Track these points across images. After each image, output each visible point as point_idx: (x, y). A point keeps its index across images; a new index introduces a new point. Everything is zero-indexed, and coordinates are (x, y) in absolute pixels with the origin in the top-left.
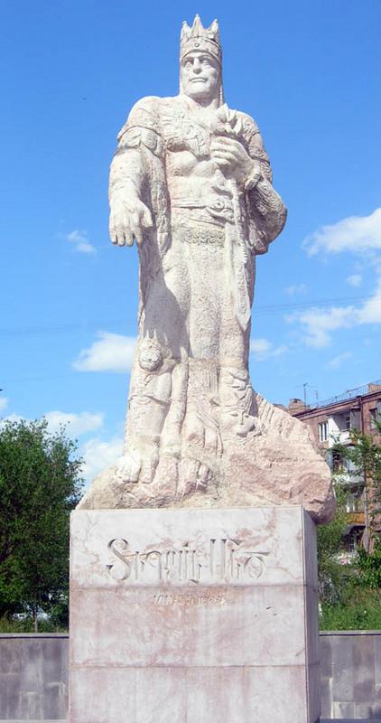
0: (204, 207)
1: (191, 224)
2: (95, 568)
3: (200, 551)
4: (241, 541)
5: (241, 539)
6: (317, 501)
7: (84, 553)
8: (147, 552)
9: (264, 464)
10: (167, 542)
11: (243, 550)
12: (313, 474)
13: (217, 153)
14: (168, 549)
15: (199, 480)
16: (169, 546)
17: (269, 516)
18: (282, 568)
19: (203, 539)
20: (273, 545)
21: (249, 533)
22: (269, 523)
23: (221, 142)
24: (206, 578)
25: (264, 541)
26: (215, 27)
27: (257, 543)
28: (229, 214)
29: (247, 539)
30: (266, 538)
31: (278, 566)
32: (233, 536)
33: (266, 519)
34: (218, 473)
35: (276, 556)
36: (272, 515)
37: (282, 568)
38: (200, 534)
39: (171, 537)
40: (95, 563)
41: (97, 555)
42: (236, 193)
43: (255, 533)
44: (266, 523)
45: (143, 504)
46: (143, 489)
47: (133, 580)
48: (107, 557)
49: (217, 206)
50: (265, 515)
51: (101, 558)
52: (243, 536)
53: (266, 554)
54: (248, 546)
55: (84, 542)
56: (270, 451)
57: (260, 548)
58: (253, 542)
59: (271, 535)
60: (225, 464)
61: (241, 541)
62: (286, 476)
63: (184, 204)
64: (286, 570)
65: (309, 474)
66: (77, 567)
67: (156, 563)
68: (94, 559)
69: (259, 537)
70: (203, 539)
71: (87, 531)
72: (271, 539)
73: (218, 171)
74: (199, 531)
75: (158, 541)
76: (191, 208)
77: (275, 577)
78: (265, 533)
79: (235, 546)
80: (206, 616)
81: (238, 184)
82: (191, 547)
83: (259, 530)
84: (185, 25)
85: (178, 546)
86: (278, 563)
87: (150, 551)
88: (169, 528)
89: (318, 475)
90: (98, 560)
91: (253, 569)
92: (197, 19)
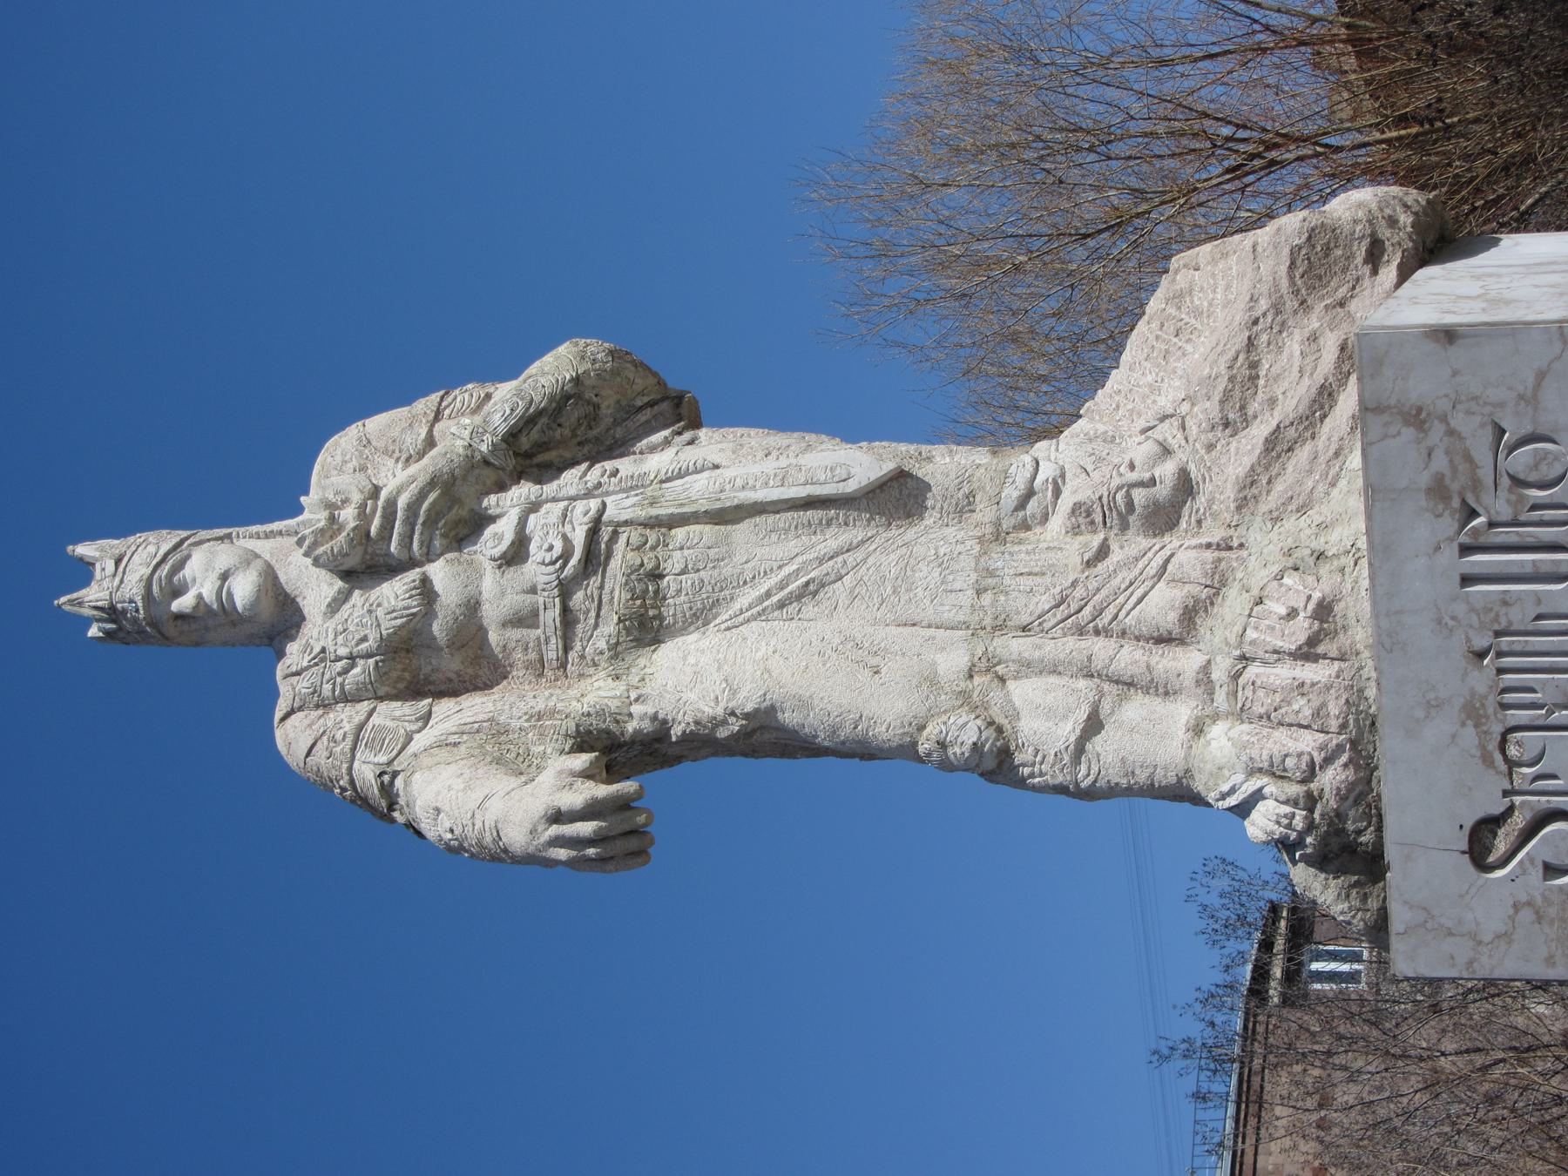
0: (561, 584)
1: (609, 627)
2: (1552, 912)
3: (1496, 619)
4: (1464, 501)
5: (1456, 503)
7: (1510, 943)
8: (1503, 767)
10: (1473, 713)
11: (1488, 498)
15: (1302, 614)
16: (1483, 705)
17: (1386, 425)
19: (1460, 609)
20: (1469, 413)
22: (1407, 423)
25: (1460, 437)
26: (84, 550)
27: (1468, 458)
30: (1451, 432)
32: (1448, 524)
33: (1399, 433)
34: (1289, 553)
35: (1501, 405)
36: (1385, 417)
38: (1447, 619)
39: (1458, 702)
40: (1537, 913)
41: (1516, 907)
42: (523, 491)
43: (1440, 463)
44: (1409, 433)
49: (558, 550)
50: (1385, 436)
51: (1523, 898)
54: (1476, 485)
55: (1480, 943)
56: (1226, 397)
57: (1483, 456)
58: (1462, 467)
59: (1444, 419)
61: (1464, 501)
62: (1296, 349)
63: (555, 644)
64: (1541, 376)
65: (1291, 278)
66: (1550, 961)
68: (1526, 915)
69: (1447, 452)
70: (1460, 609)
71: (1451, 934)
72: (1457, 421)
74: (1439, 622)
75: (1469, 735)
78: (1437, 431)
82: (1480, 642)
85: (1481, 679)
86: (1521, 397)
87: (1498, 757)
88: (1433, 706)
89: (1294, 252)
90: (1529, 904)
91: (1544, 467)
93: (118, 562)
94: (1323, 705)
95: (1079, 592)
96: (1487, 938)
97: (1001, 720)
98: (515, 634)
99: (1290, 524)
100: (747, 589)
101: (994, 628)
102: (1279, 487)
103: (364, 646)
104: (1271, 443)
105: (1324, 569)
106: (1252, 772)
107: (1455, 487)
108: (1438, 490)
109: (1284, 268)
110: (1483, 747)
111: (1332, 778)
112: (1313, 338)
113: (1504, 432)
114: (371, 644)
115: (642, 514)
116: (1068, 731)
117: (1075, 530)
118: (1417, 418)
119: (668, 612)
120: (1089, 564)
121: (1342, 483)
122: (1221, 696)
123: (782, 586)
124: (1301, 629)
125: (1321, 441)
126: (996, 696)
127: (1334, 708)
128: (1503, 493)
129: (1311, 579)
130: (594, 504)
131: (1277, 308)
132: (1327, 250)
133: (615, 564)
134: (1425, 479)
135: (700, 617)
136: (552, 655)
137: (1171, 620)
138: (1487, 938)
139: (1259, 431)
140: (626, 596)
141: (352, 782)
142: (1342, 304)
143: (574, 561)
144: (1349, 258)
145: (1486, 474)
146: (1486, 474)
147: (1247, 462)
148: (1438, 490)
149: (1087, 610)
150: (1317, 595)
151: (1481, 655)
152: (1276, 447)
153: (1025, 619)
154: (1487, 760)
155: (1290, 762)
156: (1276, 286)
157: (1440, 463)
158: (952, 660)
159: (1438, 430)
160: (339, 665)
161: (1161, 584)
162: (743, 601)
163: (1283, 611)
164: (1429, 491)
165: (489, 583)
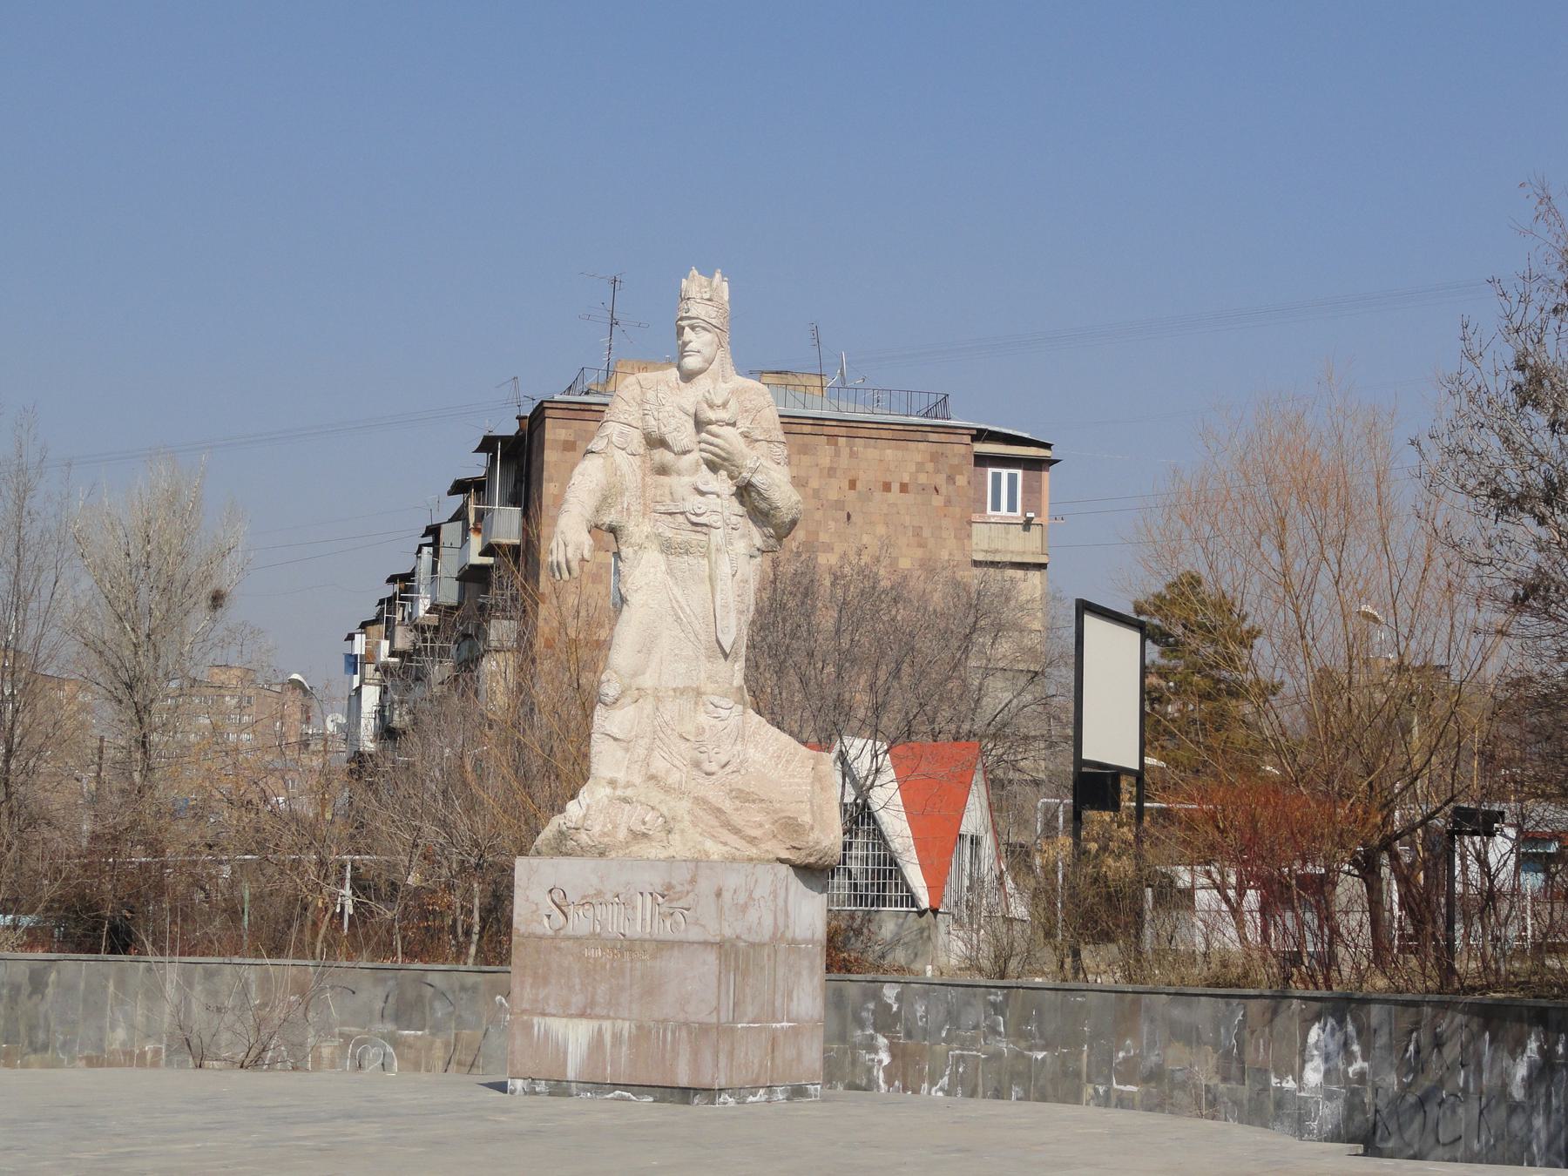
1: (669, 534)
5: (666, 893)
6: (794, 848)
9: (727, 805)
10: (599, 893)
11: (666, 904)
12: (790, 818)
13: (703, 446)
14: (600, 900)
18: (702, 926)
21: (673, 887)
23: (709, 433)
24: (635, 930)
27: (679, 899)
28: (715, 518)
29: (671, 893)
30: (688, 893)
31: (697, 923)
37: (702, 926)
41: (537, 904)
43: (679, 888)
44: (689, 877)
45: (582, 851)
46: (585, 837)
47: (569, 930)
54: (671, 901)
56: (741, 791)
57: (680, 904)
59: (692, 891)
60: (682, 807)
63: (663, 509)
65: (785, 818)
66: (519, 915)
68: (534, 907)
72: (691, 895)
73: (704, 467)
76: (670, 514)
77: (694, 934)
78: (687, 887)
80: (631, 970)
83: (682, 885)
84: (684, 280)
85: (609, 897)
89: (795, 819)
90: (538, 909)
92: (695, 272)
93: (709, 300)
94: (609, 836)
95: (669, 732)
96: (528, 892)
97: (619, 703)
98: (667, 491)
99: (687, 817)
100: (681, 591)
101: (658, 697)
103: (662, 427)
104: (719, 810)
105: (663, 834)
106: (588, 806)
107: (671, 893)
108: (670, 887)
109: (789, 814)
110: (588, 896)
111: (583, 838)
112: (761, 825)
113: (688, 909)
114: (663, 429)
116: (615, 732)
118: (693, 881)
120: (681, 736)
121: (700, 839)
122: (619, 792)
123: (681, 607)
125: (720, 830)
127: (606, 840)
128: (667, 910)
129: (659, 829)
131: (775, 811)
132: (796, 831)
133: (694, 536)
134: (674, 882)
135: (670, 571)
136: (658, 507)
137: (653, 771)
138: (528, 892)
140: (679, 541)
141: (607, 421)
142: (774, 836)
143: (694, 519)
144: (793, 840)
146: (674, 904)
147: (713, 800)
148: (670, 887)
149: (662, 735)
150: (651, 833)
151: (618, 896)
152: (718, 812)
153: (661, 709)
154: (584, 897)
155: (589, 822)
156: (782, 811)
157: (679, 888)
159: (690, 888)
160: (656, 413)
161: (669, 765)
162: (675, 590)
163: (647, 819)
164: (670, 883)
165: (686, 479)
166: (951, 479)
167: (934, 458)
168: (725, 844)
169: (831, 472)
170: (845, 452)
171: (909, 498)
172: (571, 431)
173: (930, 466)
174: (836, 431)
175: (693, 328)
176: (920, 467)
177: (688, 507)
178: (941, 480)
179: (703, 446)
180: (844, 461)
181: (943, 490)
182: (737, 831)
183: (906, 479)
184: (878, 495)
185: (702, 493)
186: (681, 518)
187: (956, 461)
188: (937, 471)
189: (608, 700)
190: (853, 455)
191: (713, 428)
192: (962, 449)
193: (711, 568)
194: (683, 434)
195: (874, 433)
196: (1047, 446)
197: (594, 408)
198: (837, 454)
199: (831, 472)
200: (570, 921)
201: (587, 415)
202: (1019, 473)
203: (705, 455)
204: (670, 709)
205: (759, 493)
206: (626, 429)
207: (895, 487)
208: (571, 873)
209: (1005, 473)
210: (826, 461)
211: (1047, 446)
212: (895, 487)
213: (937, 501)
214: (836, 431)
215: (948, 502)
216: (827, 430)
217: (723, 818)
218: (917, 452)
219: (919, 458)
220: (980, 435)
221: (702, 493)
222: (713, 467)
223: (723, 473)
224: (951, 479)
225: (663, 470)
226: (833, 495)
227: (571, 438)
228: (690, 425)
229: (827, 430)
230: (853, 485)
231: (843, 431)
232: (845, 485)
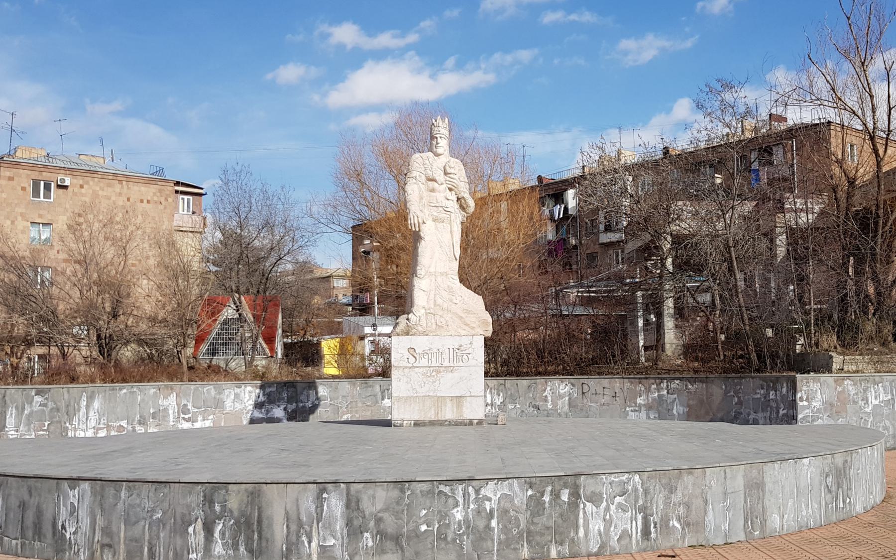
1: (436, 214)
13: (448, 182)
23: (449, 177)
31: (473, 358)
32: (457, 347)
48: (407, 355)
52: (460, 347)
53: (469, 354)
56: (467, 310)
63: (434, 205)
67: (426, 357)
68: (402, 355)
73: (448, 190)
75: (427, 348)
79: (457, 351)
81: (456, 195)
102: (456, 319)
104: (461, 317)
108: (461, 346)
111: (420, 328)
115: (452, 220)
117: (448, 287)
119: (437, 223)
124: (440, 324)
126: (427, 276)
130: (453, 212)
131: (479, 318)
137: (438, 303)
139: (463, 315)
143: (446, 209)
145: (463, 352)
146: (463, 352)
147: (459, 313)
158: (432, 270)
165: (442, 195)
166: (166, 199)
167: (160, 191)
168: (465, 330)
169: (120, 194)
170: (125, 187)
171: (150, 206)
172: (12, 173)
173: (158, 194)
174: (122, 179)
175: (441, 137)
176: (154, 194)
177: (444, 205)
178: (162, 199)
179: (448, 182)
180: (125, 190)
181: (163, 203)
182: (467, 324)
183: (149, 198)
184: (139, 204)
185: (448, 200)
186: (441, 209)
187: (168, 193)
188: (161, 196)
189: (421, 276)
190: (129, 188)
191: (451, 176)
192: (170, 188)
193: (451, 228)
194: (440, 177)
195: (137, 181)
196: (202, 189)
197: (49, 167)
198: (122, 187)
199: (120, 194)
200: (418, 360)
201: (19, 167)
202: (191, 198)
203: (449, 186)
204: (439, 279)
205: (465, 201)
206: (421, 174)
207: (145, 201)
208: (420, 343)
209: (186, 197)
210: (118, 190)
211: (202, 189)
212: (145, 201)
213: (162, 207)
214: (122, 179)
215: (165, 208)
216: (119, 178)
217: (463, 320)
218: (153, 189)
219: (154, 191)
220: (178, 183)
221: (448, 200)
222: (450, 190)
223: (453, 192)
224: (166, 199)
225: (433, 190)
226: (121, 203)
227: (12, 176)
228: (442, 173)
229: (119, 178)
230: (128, 200)
231: (125, 179)
232: (126, 200)
